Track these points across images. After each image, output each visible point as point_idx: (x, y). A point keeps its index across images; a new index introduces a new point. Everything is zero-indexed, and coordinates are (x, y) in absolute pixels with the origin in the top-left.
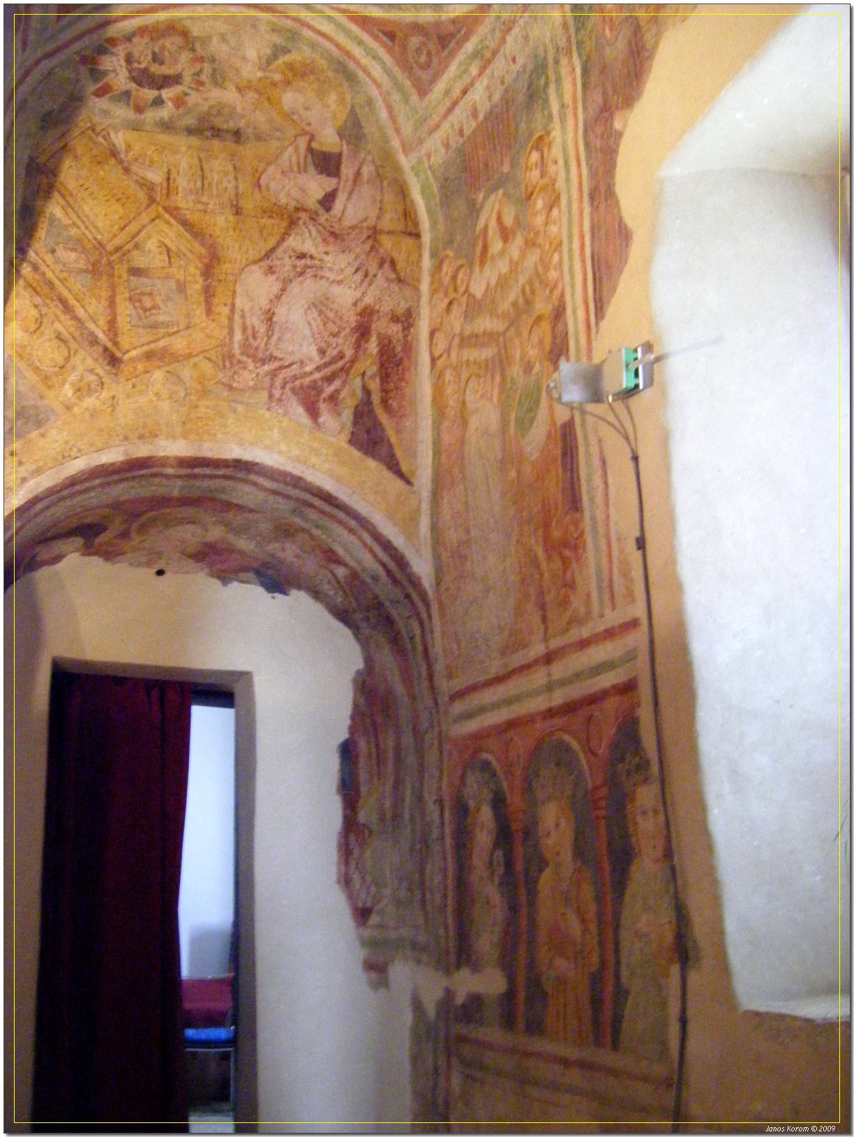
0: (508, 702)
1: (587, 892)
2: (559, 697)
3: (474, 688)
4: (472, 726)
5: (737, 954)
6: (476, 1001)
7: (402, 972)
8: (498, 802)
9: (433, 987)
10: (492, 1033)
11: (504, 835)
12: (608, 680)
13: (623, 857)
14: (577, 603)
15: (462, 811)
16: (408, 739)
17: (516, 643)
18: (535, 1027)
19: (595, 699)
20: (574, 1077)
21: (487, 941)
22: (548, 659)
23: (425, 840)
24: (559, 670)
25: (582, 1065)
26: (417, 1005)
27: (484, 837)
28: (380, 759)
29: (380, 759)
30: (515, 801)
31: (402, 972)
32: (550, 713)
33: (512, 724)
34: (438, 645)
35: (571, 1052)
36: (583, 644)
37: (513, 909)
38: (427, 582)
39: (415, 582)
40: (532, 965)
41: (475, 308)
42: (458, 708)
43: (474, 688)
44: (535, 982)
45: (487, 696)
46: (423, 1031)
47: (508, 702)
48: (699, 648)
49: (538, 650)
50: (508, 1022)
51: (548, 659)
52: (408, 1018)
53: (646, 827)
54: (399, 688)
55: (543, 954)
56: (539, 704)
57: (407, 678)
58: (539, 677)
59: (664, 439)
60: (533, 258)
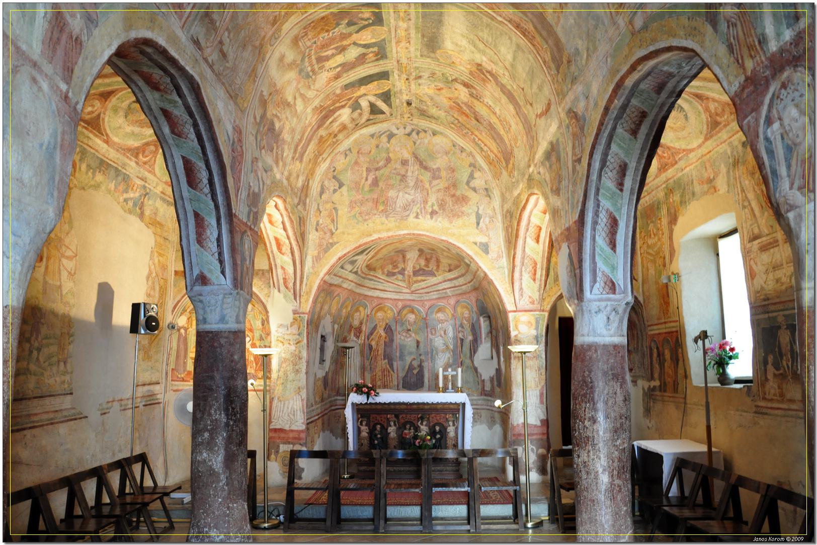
0: (659, 329)
1: (673, 366)
2: (667, 330)
3: (652, 325)
4: (652, 332)
5: (693, 377)
6: (655, 387)
7: (640, 383)
8: (658, 348)
9: (646, 385)
10: (658, 393)
11: (659, 355)
12: (674, 329)
13: (678, 360)
14: (669, 315)
15: (651, 349)
16: (639, 333)
17: (659, 319)
18: (665, 391)
19: (672, 332)
20: (671, 399)
21: (656, 375)
22: (665, 323)
23: (644, 354)
24: (667, 325)
25: (673, 397)
26: (643, 389)
27: (655, 355)
28: (633, 336)
29: (633, 336)
30: (661, 348)
31: (640, 383)
32: (666, 333)
33: (659, 334)
34: (645, 315)
35: (671, 395)
36: (670, 322)
37: (661, 369)
38: (642, 302)
39: (640, 302)
40: (664, 379)
41: (649, 247)
42: (649, 328)
43: (652, 325)
44: (665, 383)
45: (655, 327)
46: (645, 394)
47: (659, 329)
48: (686, 327)
49: (663, 321)
50: (660, 391)
51: (665, 323)
52: (641, 392)
53: (680, 355)
54: (637, 322)
55: (666, 377)
56: (664, 331)
57: (639, 320)
58: (663, 326)
59: (681, 291)
60: (659, 243)
